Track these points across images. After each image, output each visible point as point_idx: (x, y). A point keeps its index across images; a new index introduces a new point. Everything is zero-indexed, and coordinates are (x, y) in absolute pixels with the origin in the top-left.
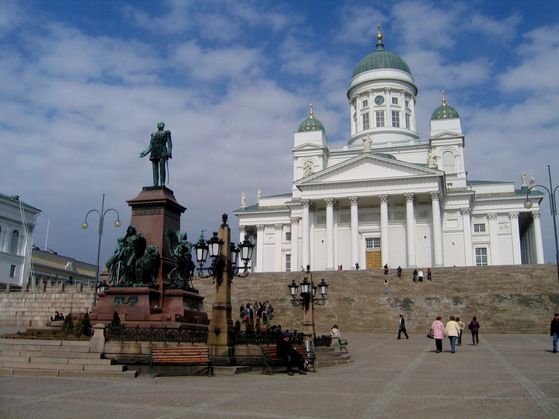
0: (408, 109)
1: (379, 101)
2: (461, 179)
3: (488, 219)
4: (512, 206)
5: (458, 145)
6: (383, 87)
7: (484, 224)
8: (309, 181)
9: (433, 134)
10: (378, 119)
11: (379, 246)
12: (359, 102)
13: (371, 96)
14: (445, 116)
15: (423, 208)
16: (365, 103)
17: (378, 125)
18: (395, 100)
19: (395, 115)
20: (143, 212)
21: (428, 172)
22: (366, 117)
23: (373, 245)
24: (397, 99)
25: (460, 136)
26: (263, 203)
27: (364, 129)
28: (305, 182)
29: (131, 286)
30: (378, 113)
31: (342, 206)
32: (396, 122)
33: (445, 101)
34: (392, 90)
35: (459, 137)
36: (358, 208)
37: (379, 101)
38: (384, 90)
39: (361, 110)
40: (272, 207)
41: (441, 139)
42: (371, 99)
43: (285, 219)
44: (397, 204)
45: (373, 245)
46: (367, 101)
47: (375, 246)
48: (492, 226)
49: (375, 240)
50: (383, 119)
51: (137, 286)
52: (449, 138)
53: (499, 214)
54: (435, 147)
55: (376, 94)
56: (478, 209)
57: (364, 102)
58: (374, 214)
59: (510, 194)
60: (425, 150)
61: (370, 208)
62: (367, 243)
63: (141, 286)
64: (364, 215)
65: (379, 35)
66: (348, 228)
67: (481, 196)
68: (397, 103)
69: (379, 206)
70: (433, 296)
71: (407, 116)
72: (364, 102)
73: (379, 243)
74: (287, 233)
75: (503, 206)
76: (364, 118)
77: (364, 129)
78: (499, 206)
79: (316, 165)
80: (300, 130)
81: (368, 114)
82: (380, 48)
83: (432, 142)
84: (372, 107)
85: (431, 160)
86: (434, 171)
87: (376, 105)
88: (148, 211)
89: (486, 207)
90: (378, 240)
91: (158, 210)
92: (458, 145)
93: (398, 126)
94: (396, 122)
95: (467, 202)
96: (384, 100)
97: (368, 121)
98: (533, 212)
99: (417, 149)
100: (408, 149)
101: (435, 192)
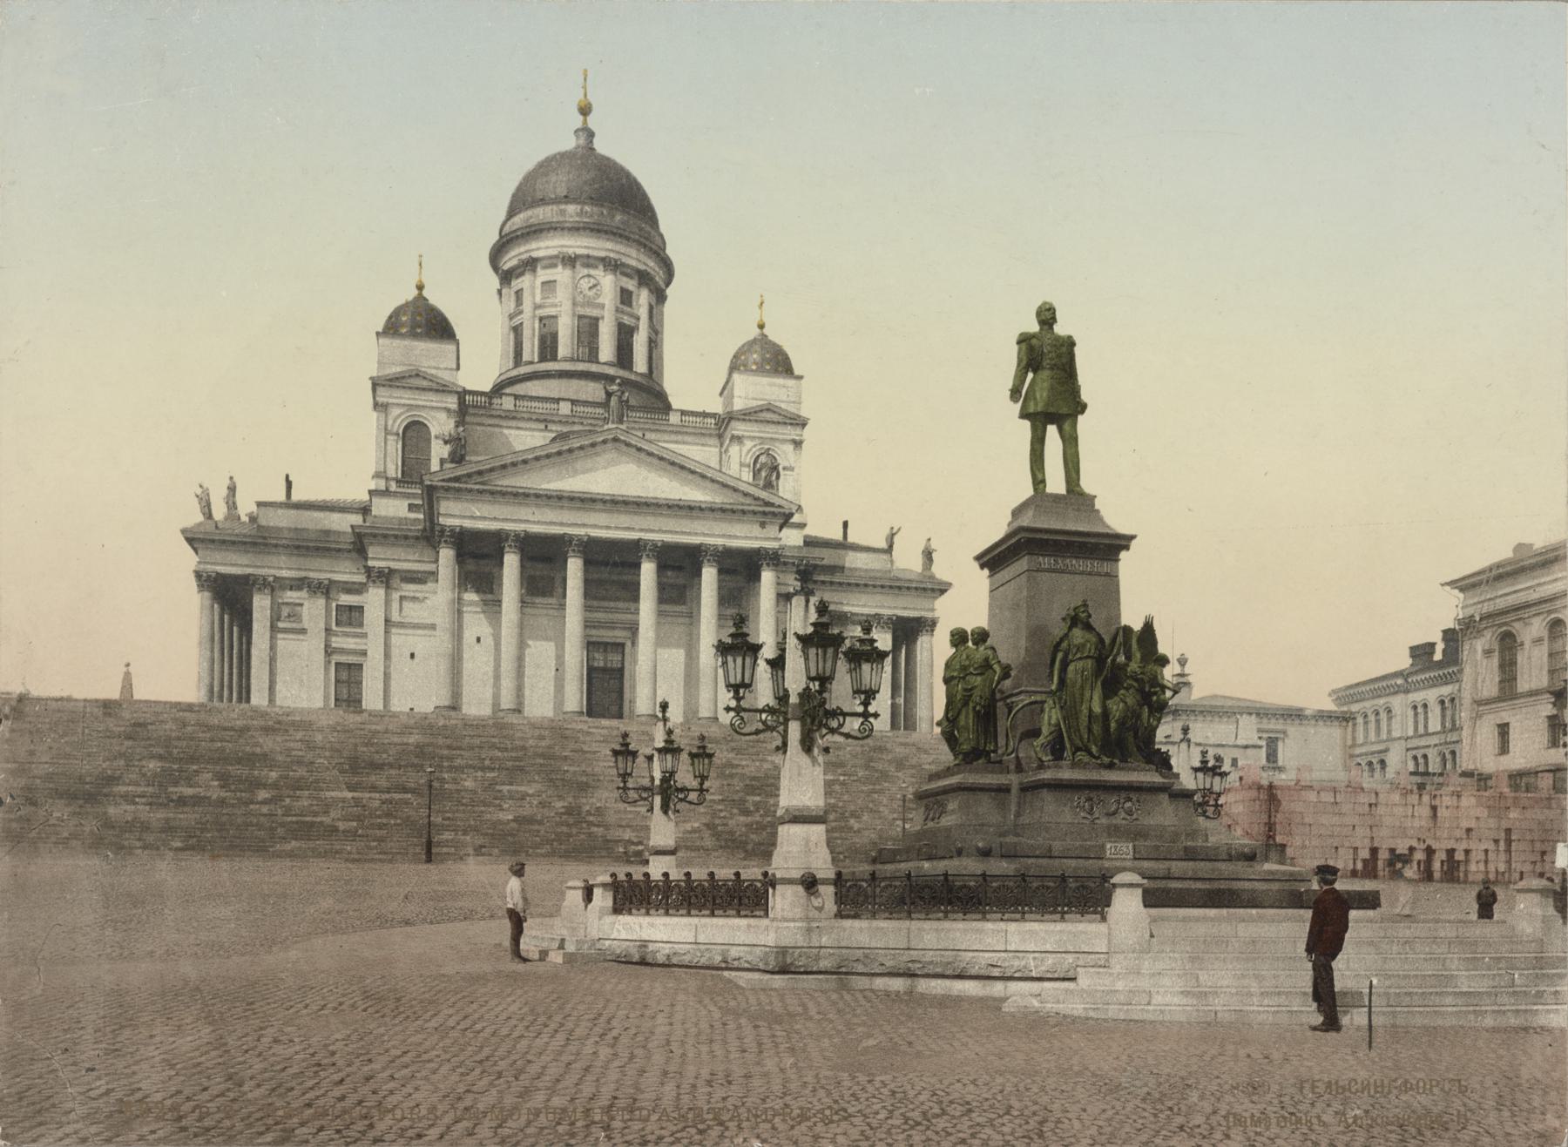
8: (457, 479)
9: (738, 405)
24: (630, 293)
27: (543, 359)
28: (450, 480)
43: (346, 572)
44: (680, 565)
64: (600, 582)
77: (543, 359)
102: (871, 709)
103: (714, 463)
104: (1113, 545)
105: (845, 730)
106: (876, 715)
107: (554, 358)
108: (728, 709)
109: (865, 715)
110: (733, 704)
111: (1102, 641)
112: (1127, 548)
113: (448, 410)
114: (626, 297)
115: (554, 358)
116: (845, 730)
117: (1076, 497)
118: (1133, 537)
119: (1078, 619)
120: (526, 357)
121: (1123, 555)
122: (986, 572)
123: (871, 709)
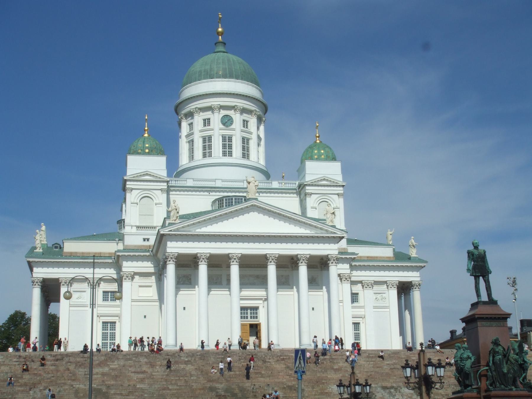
0: (259, 138)
1: (227, 121)
3: (363, 286)
4: (392, 273)
5: (338, 194)
6: (233, 104)
7: (357, 294)
8: (177, 230)
9: (308, 178)
10: (224, 146)
11: (257, 317)
12: (198, 120)
13: (216, 114)
14: (323, 157)
16: (207, 122)
17: (224, 154)
18: (245, 123)
19: (245, 141)
20: (489, 323)
21: (326, 231)
22: (207, 141)
23: (249, 315)
24: (247, 122)
25: (341, 184)
26: (69, 247)
29: (511, 390)
30: (224, 138)
31: (219, 265)
33: (319, 137)
34: (244, 111)
35: (340, 186)
36: (240, 267)
37: (227, 121)
39: (201, 131)
40: (83, 253)
41: (318, 186)
42: (216, 118)
45: (249, 315)
46: (209, 119)
47: (251, 318)
48: (367, 296)
49: (251, 310)
50: (230, 147)
51: (517, 390)
52: (327, 186)
53: (377, 283)
54: (311, 194)
55: (224, 112)
56: (358, 275)
57: (204, 120)
58: (250, 276)
59: (388, 259)
60: (292, 195)
61: (253, 270)
62: (241, 313)
63: (521, 390)
65: (220, 30)
66: (228, 293)
67: (361, 259)
68: (247, 128)
69: (265, 267)
70: (389, 385)
71: (259, 145)
72: (204, 120)
73: (257, 313)
74: (104, 292)
75: (382, 273)
76: (204, 140)
77: (204, 156)
78: (377, 273)
79: (158, 202)
80: (136, 153)
81: (210, 138)
82: (221, 48)
84: (217, 130)
85: (329, 215)
87: (222, 126)
88: (494, 323)
89: (363, 273)
90: (257, 308)
91: (501, 323)
92: (338, 194)
96: (233, 121)
97: (210, 147)
98: (413, 283)
99: (282, 193)
100: (270, 193)
101: (334, 256)
102: (442, 381)
103: (298, 211)
104: (505, 317)
105: (436, 387)
106: (444, 383)
108: (406, 383)
109: (441, 383)
110: (407, 381)
111: (504, 349)
112: (509, 317)
113: (161, 190)
114: (245, 123)
116: (436, 387)
117: (492, 302)
118: (510, 315)
119: (496, 343)
120: (195, 157)
121: (508, 319)
123: (442, 381)
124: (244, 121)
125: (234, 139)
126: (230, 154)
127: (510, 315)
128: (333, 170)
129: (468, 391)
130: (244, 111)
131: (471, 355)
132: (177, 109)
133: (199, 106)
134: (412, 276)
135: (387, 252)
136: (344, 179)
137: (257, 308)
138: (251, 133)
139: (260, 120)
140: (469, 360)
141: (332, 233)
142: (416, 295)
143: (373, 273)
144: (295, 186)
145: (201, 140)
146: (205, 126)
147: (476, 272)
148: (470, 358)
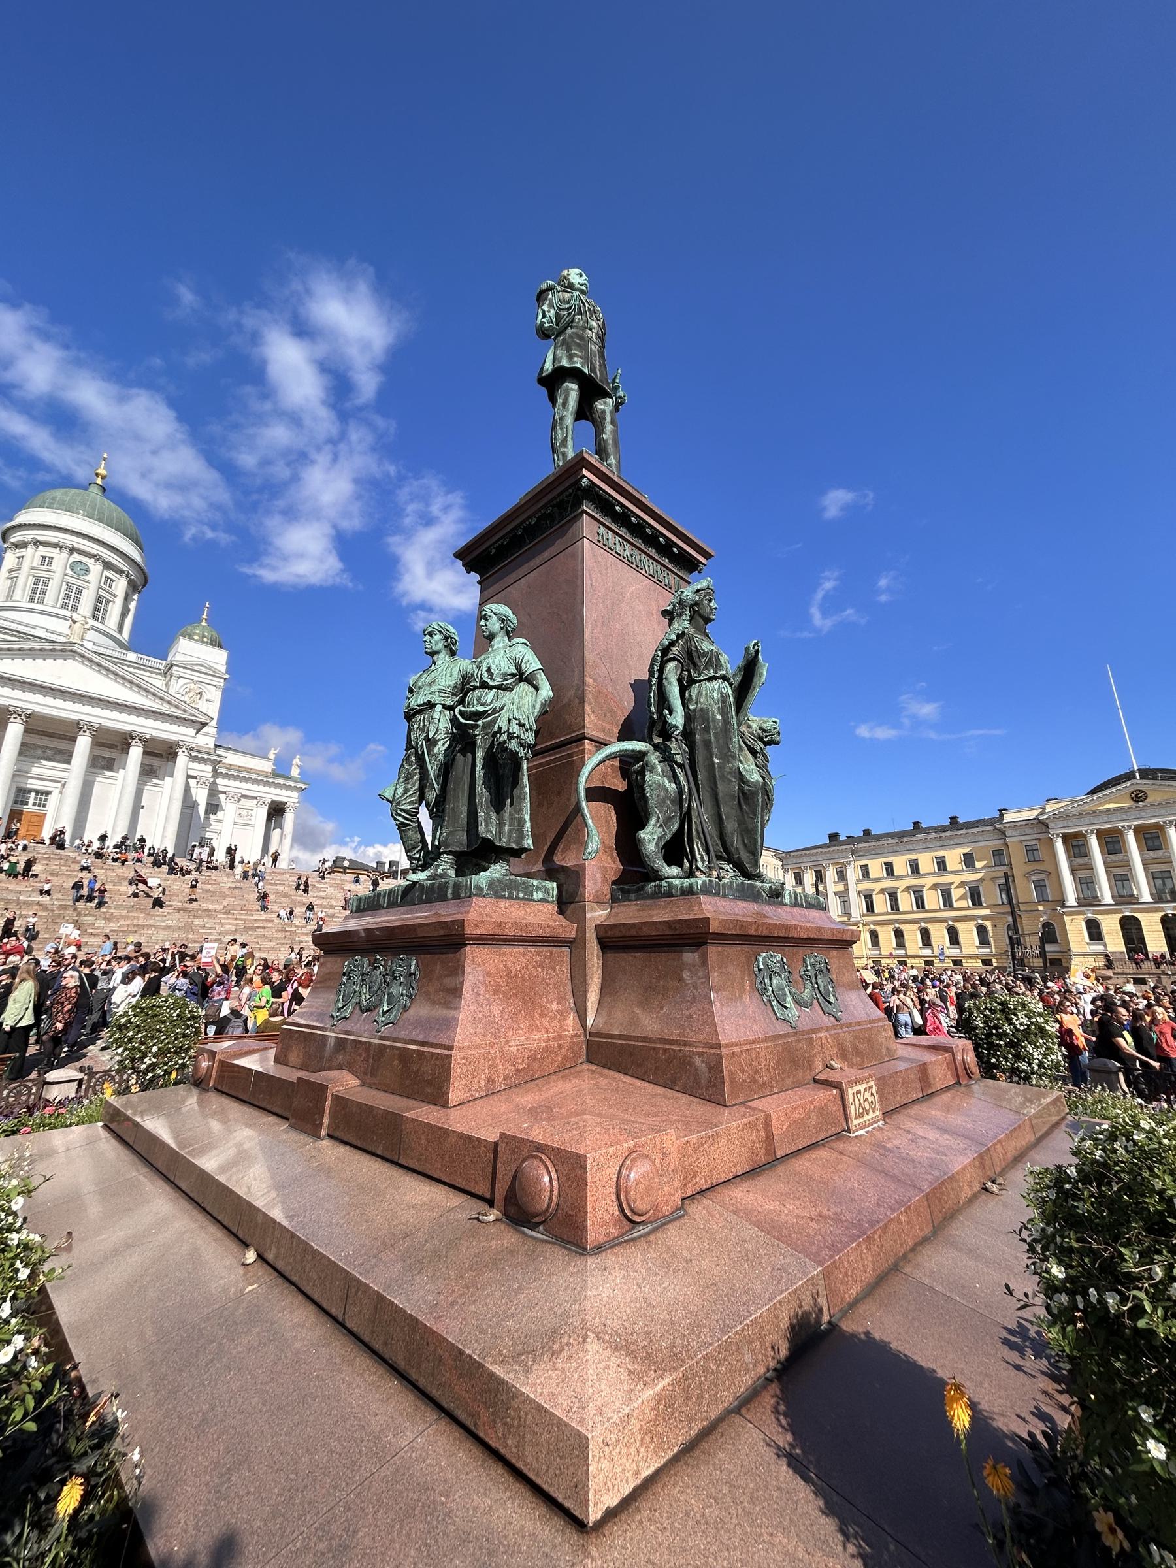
2: (208, 735)
6: (95, 552)
11: (44, 806)
15: (154, 762)
16: (47, 561)
24: (112, 581)
27: (31, 601)
32: (98, 611)
34: (108, 565)
38: (95, 557)
47: (34, 804)
58: (48, 748)
69: (74, 740)
73: (46, 800)
76: (37, 582)
77: (31, 601)
83: (175, 668)
86: (195, 712)
89: (232, 783)
93: (103, 622)
94: (98, 611)
95: (209, 768)
107: (41, 601)
115: (41, 601)
122: (475, 577)
124: (107, 577)
125: (85, 592)
126: (75, 609)
127: (707, 556)
128: (219, 658)
129: (498, 890)
130: (108, 565)
131: (533, 664)
132: (5, 535)
133: (39, 538)
134: (290, 797)
135: (266, 766)
136: (227, 672)
137: (48, 793)
138: (115, 596)
139: (133, 587)
140: (523, 687)
141: (191, 715)
142: (289, 818)
143: (243, 785)
144: (162, 667)
145: (31, 580)
146: (43, 563)
147: (571, 358)
148: (530, 680)
